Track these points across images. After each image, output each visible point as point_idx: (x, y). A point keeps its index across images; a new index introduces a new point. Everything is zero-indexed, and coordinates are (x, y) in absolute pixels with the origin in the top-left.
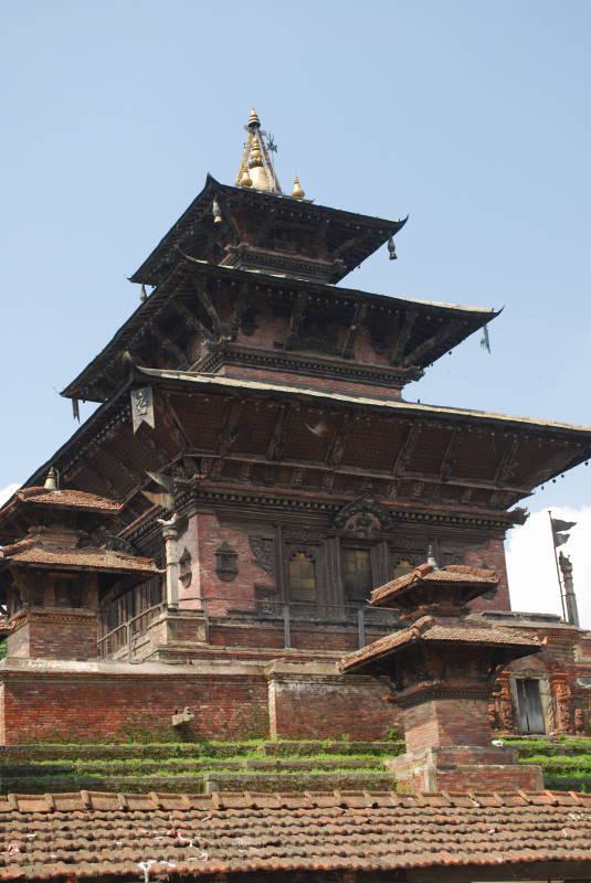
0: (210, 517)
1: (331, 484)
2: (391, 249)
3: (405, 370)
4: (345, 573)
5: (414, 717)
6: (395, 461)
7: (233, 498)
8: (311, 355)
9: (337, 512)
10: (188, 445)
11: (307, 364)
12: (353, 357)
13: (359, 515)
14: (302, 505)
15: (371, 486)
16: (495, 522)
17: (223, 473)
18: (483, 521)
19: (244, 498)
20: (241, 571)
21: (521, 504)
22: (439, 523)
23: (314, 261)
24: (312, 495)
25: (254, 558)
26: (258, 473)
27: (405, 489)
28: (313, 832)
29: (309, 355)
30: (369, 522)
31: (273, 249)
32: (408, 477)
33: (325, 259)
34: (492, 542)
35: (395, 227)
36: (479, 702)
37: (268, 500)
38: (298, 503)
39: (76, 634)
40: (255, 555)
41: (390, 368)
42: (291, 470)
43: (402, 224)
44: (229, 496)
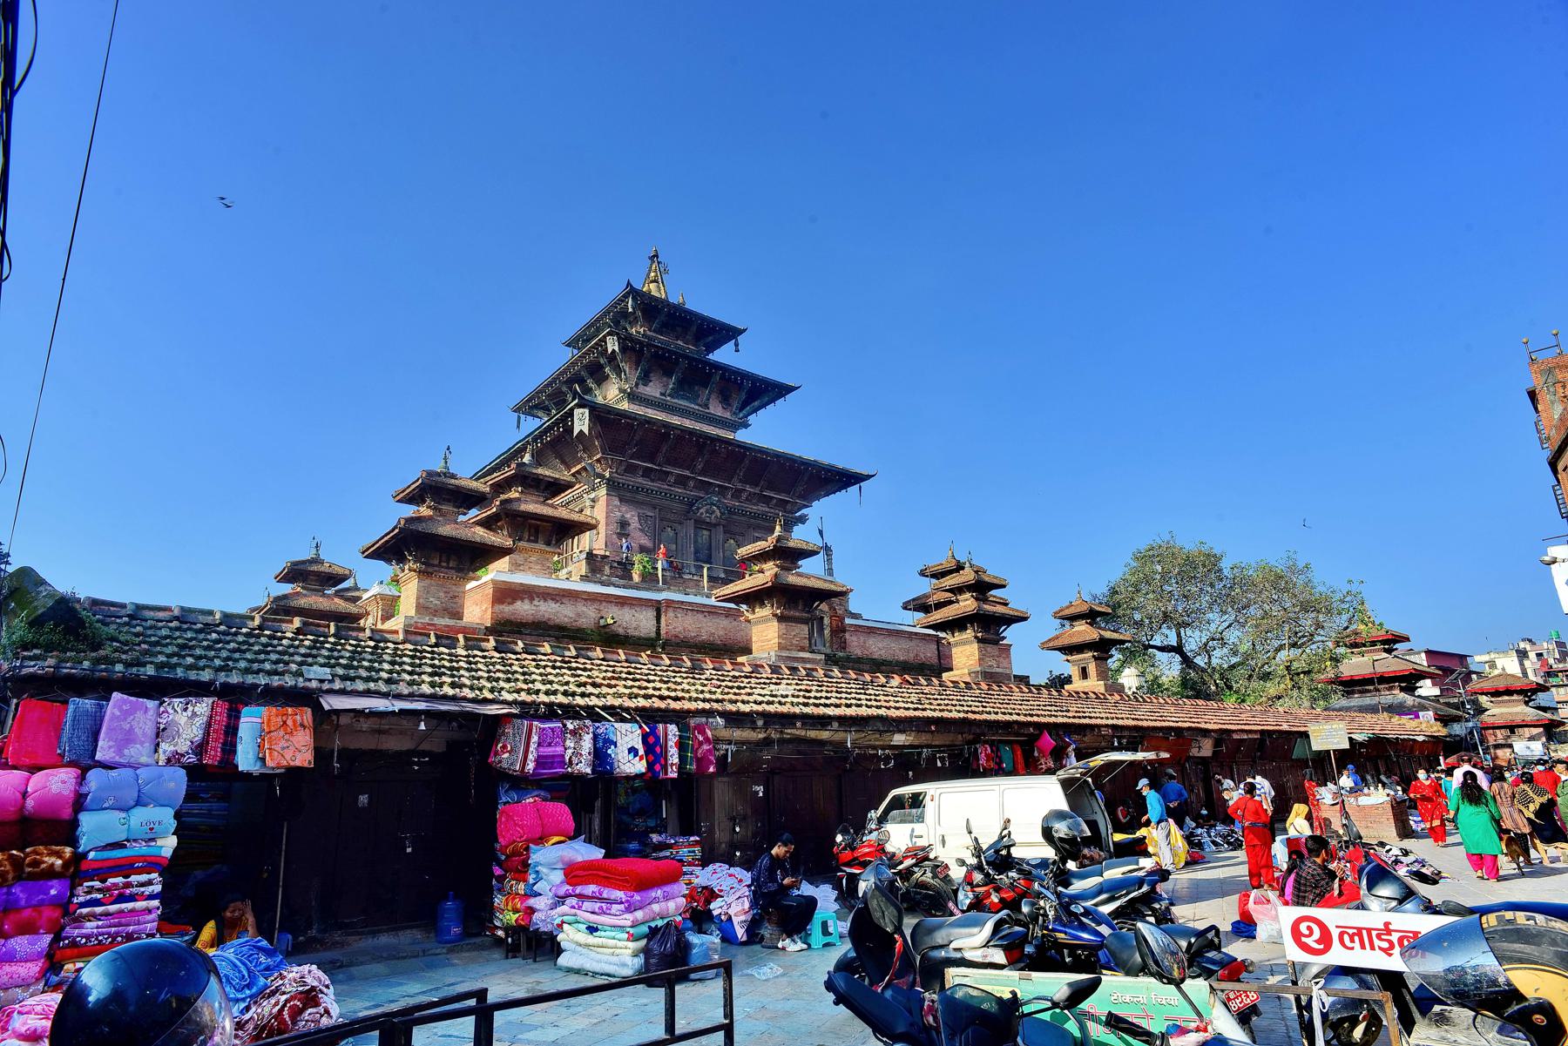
2: (737, 345)
4: (696, 542)
7: (630, 487)
9: (693, 505)
12: (708, 409)
13: (709, 506)
17: (625, 471)
20: (632, 534)
21: (804, 511)
22: (754, 518)
24: (680, 491)
26: (647, 473)
27: (737, 494)
30: (714, 512)
32: (739, 486)
37: (652, 491)
38: (671, 495)
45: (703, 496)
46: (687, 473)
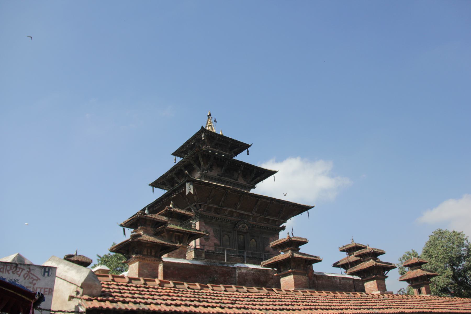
0: (202, 222)
1: (235, 215)
2: (248, 152)
3: (251, 185)
5: (285, 280)
6: (253, 210)
7: (209, 217)
8: (226, 178)
9: (236, 224)
10: (198, 200)
11: (226, 181)
13: (243, 224)
14: (227, 220)
15: (246, 217)
16: (277, 229)
18: (274, 229)
19: (212, 217)
21: (284, 224)
23: (226, 153)
25: (214, 235)
28: (325, 305)
29: (227, 179)
30: (245, 227)
31: (215, 149)
32: (255, 214)
33: (229, 153)
34: (276, 235)
35: (249, 146)
36: (304, 276)
38: (226, 220)
39: (181, 252)
40: (214, 234)
41: (247, 184)
42: (225, 210)
43: (251, 145)
44: (208, 216)
45: (240, 220)
46: (233, 210)
